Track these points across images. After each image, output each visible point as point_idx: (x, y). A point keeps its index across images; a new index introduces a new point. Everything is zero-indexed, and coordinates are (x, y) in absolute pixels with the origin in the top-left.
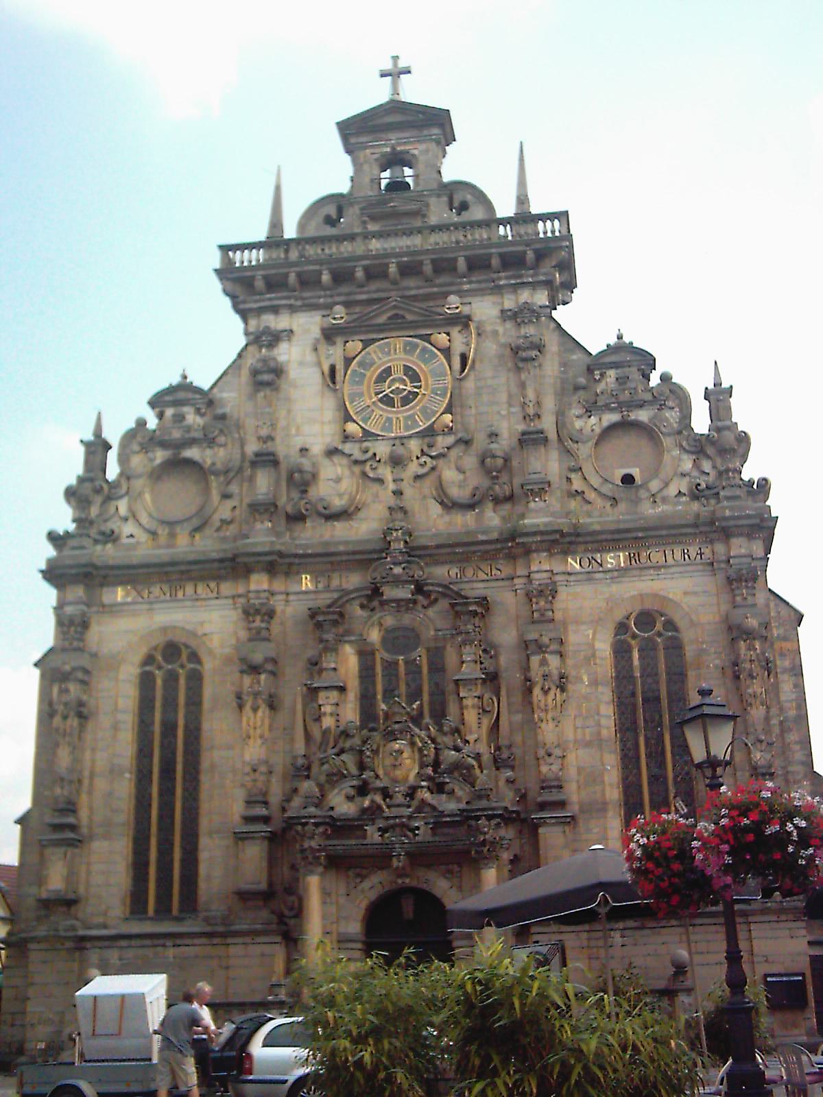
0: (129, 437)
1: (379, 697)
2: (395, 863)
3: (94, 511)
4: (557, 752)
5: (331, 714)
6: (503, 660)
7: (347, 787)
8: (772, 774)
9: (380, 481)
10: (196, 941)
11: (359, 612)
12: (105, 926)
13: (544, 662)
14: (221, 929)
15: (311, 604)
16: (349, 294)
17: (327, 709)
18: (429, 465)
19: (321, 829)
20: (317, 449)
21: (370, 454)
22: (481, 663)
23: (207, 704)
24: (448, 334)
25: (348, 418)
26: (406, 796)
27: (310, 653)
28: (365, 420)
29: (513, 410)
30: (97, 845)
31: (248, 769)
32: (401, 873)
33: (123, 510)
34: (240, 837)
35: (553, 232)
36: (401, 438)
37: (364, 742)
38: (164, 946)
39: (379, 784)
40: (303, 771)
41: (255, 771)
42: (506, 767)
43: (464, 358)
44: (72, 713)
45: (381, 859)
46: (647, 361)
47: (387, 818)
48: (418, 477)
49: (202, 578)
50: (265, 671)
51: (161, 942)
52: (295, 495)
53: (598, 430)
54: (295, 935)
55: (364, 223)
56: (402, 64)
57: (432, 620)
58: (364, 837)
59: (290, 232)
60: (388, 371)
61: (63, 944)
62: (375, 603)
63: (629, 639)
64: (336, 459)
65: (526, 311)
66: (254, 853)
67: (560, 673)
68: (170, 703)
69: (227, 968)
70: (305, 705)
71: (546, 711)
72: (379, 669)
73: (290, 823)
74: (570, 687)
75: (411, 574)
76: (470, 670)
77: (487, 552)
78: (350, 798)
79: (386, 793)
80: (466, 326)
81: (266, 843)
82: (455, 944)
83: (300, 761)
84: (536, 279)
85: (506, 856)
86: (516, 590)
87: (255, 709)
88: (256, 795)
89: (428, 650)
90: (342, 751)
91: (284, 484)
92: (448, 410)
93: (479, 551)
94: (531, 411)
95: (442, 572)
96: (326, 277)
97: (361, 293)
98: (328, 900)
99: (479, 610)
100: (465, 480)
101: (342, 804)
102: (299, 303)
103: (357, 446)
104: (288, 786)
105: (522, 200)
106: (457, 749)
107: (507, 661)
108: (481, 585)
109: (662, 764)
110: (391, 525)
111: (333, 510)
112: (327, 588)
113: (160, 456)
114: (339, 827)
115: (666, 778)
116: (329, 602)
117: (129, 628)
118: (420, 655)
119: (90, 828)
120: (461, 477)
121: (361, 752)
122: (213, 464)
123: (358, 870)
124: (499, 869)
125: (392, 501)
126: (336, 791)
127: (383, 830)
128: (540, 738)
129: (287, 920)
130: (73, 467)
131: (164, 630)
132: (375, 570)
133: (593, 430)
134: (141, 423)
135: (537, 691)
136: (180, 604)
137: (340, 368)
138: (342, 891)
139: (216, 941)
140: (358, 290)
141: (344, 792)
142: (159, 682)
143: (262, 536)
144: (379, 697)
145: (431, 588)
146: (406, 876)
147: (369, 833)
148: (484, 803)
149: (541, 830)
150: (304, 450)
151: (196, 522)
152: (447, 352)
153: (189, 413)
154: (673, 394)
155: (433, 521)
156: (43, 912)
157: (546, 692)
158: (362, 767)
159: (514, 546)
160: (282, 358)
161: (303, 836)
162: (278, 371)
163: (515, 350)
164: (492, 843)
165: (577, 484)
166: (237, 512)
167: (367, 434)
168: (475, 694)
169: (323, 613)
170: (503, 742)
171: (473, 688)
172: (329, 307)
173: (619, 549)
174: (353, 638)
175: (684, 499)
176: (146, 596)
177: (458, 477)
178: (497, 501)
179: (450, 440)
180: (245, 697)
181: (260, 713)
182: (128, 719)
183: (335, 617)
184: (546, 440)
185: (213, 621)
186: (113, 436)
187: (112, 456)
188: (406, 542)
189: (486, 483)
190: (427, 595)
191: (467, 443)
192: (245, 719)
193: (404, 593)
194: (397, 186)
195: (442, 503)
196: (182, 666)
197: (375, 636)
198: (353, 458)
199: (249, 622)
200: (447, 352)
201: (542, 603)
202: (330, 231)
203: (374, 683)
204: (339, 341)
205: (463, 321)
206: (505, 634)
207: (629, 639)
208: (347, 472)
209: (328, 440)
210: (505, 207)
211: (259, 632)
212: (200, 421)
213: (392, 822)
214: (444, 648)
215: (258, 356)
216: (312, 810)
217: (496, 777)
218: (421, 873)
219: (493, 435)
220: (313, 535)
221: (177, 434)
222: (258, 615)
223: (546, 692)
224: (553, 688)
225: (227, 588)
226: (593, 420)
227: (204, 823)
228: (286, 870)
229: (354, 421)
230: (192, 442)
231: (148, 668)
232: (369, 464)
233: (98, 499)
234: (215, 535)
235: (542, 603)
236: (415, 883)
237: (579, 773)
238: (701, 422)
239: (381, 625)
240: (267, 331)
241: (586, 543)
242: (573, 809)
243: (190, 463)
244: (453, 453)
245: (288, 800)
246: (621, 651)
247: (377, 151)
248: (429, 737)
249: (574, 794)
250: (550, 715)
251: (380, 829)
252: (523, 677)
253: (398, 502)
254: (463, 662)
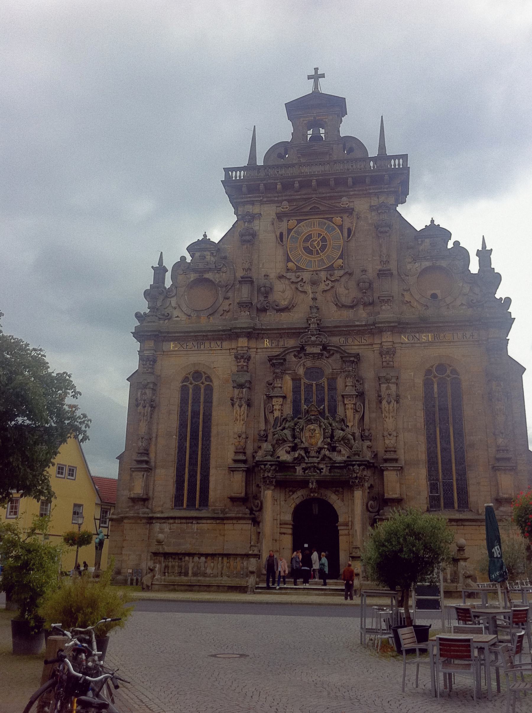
0: (176, 266)
1: (303, 402)
2: (311, 486)
3: (159, 303)
4: (395, 434)
5: (279, 410)
6: (366, 386)
7: (287, 447)
8: (507, 450)
9: (305, 292)
10: (209, 521)
11: (294, 359)
12: (162, 512)
13: (388, 388)
14: (221, 516)
15: (270, 354)
16: (290, 196)
17: (277, 407)
18: (330, 285)
19: (274, 467)
20: (273, 275)
21: (300, 279)
22: (356, 387)
23: (215, 403)
24: (341, 217)
25: (289, 260)
26: (317, 452)
27: (270, 378)
28: (298, 261)
29: (374, 258)
30: (158, 471)
31: (236, 436)
32: (312, 491)
33: (174, 304)
34: (232, 470)
35: (399, 165)
36: (316, 271)
37: (296, 425)
38: (192, 523)
39: (303, 446)
40: (264, 438)
41: (239, 437)
42: (367, 440)
43: (349, 230)
44: (147, 405)
45: (303, 484)
46: (447, 235)
47: (307, 463)
48: (325, 291)
49: (214, 339)
50: (245, 387)
51: (191, 521)
52: (262, 299)
53: (419, 271)
54: (258, 520)
55: (299, 157)
56: (319, 72)
57: (330, 365)
58: (295, 472)
59: (260, 162)
60: (310, 236)
61: (141, 520)
62: (302, 355)
63: (433, 378)
64: (283, 280)
65: (383, 207)
66: (239, 478)
67: (397, 394)
68: (196, 400)
69: (224, 535)
70: (265, 405)
71: (389, 413)
72: (303, 388)
73: (258, 464)
74: (401, 401)
75: (321, 340)
76: (350, 391)
77: (359, 330)
78: (288, 453)
79: (306, 450)
80: (351, 214)
81: (244, 473)
82: (339, 528)
83: (262, 433)
84: (389, 190)
85: (367, 485)
86: (374, 351)
87: (240, 406)
88: (240, 449)
89: (328, 379)
90: (284, 428)
91: (256, 293)
92: (341, 257)
93: (355, 330)
94: (385, 260)
95: (336, 340)
96: (279, 186)
97: (297, 195)
98: (276, 503)
99: (356, 360)
100: (349, 293)
101: (284, 456)
102: (265, 199)
103: (294, 274)
104: (256, 445)
105: (382, 146)
106: (343, 430)
107: (369, 387)
108: (355, 347)
109: (449, 443)
110: (310, 316)
111: (281, 307)
112: (277, 346)
113: (193, 276)
114: (282, 466)
115: (450, 449)
116: (277, 353)
117: (177, 362)
118: (324, 381)
119: (155, 463)
120: (347, 292)
121: (294, 430)
122: (220, 282)
123: (291, 489)
124: (363, 492)
125: (311, 303)
126: (281, 448)
127: (304, 469)
128: (385, 426)
129: (254, 512)
130: (148, 280)
131: (194, 365)
132: (302, 338)
133: (416, 270)
134: (183, 258)
135: (384, 402)
136: (202, 352)
137: (285, 233)
138: (282, 499)
139: (218, 521)
140: (295, 194)
141: (285, 449)
142: (191, 391)
143: (244, 320)
144: (303, 402)
145: (331, 348)
146: (316, 493)
147: (298, 470)
148: (357, 458)
149: (385, 473)
150: (266, 276)
151: (210, 311)
152: (341, 227)
153: (207, 255)
154: (460, 253)
155: (333, 315)
156: (131, 504)
157: (389, 403)
158: (294, 437)
159: (373, 329)
160: (256, 228)
161: (264, 471)
162: (254, 235)
163: (377, 227)
164: (360, 478)
165: (407, 298)
166: (231, 307)
167: (299, 269)
168: (353, 402)
169: (276, 359)
170: (366, 427)
171: (351, 399)
172: (281, 202)
173: (429, 332)
174: (290, 372)
175: (464, 307)
176: (185, 347)
177: (347, 292)
178: (365, 305)
179: (342, 272)
180: (235, 400)
181: (242, 409)
182: (175, 409)
183: (282, 361)
184: (392, 274)
185: (220, 362)
186: (169, 264)
187: (168, 275)
188: (318, 324)
189: (360, 295)
190: (329, 351)
191: (351, 274)
192: (235, 411)
193: (317, 350)
194: (316, 138)
195: (336, 305)
196: (203, 383)
197: (301, 371)
198: (291, 280)
199: (238, 362)
200: (341, 227)
201: (388, 358)
202: (282, 162)
203: (300, 395)
204: (285, 220)
205: (350, 211)
206: (368, 373)
207: (433, 378)
208: (288, 288)
209: (278, 271)
210: (373, 152)
211: (242, 368)
212: (212, 259)
213: (309, 465)
214: (337, 378)
215: (243, 227)
216: (269, 458)
217: (362, 445)
218: (322, 491)
219: (364, 271)
220: (271, 319)
221: (201, 266)
222: (243, 358)
223: (389, 403)
224: (393, 401)
225: (226, 345)
226: (417, 265)
227: (213, 463)
228: (254, 488)
229: (292, 261)
230: (210, 270)
231: (185, 384)
232: (299, 284)
233: (161, 298)
234: (220, 317)
235: (388, 358)
236: (319, 496)
237: (405, 445)
238: (474, 267)
239: (304, 365)
240: (248, 214)
241: (411, 328)
242: (402, 463)
243: (207, 280)
244: (343, 280)
245: (256, 452)
246: (428, 384)
247: (307, 119)
248: (329, 423)
249: (401, 455)
250: (391, 414)
251: (303, 468)
252: (377, 395)
253: (314, 304)
254: (346, 386)
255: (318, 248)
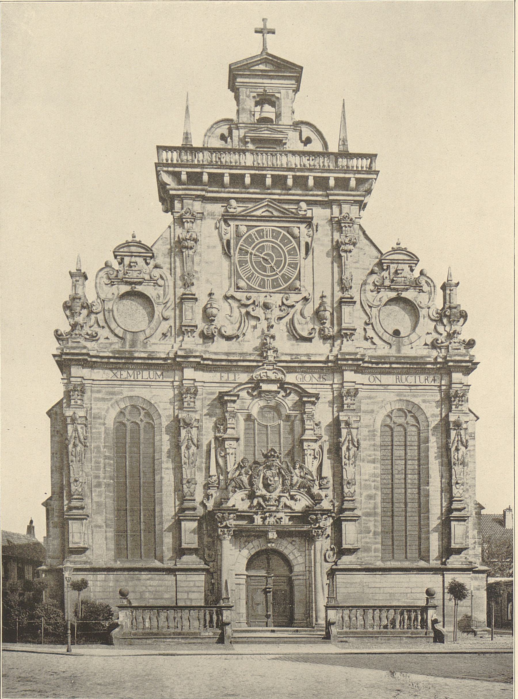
21: (251, 301)
71: (349, 460)
105: (344, 141)
149: (344, 523)
190: (285, 390)
250: (351, 462)
255: (273, 264)
